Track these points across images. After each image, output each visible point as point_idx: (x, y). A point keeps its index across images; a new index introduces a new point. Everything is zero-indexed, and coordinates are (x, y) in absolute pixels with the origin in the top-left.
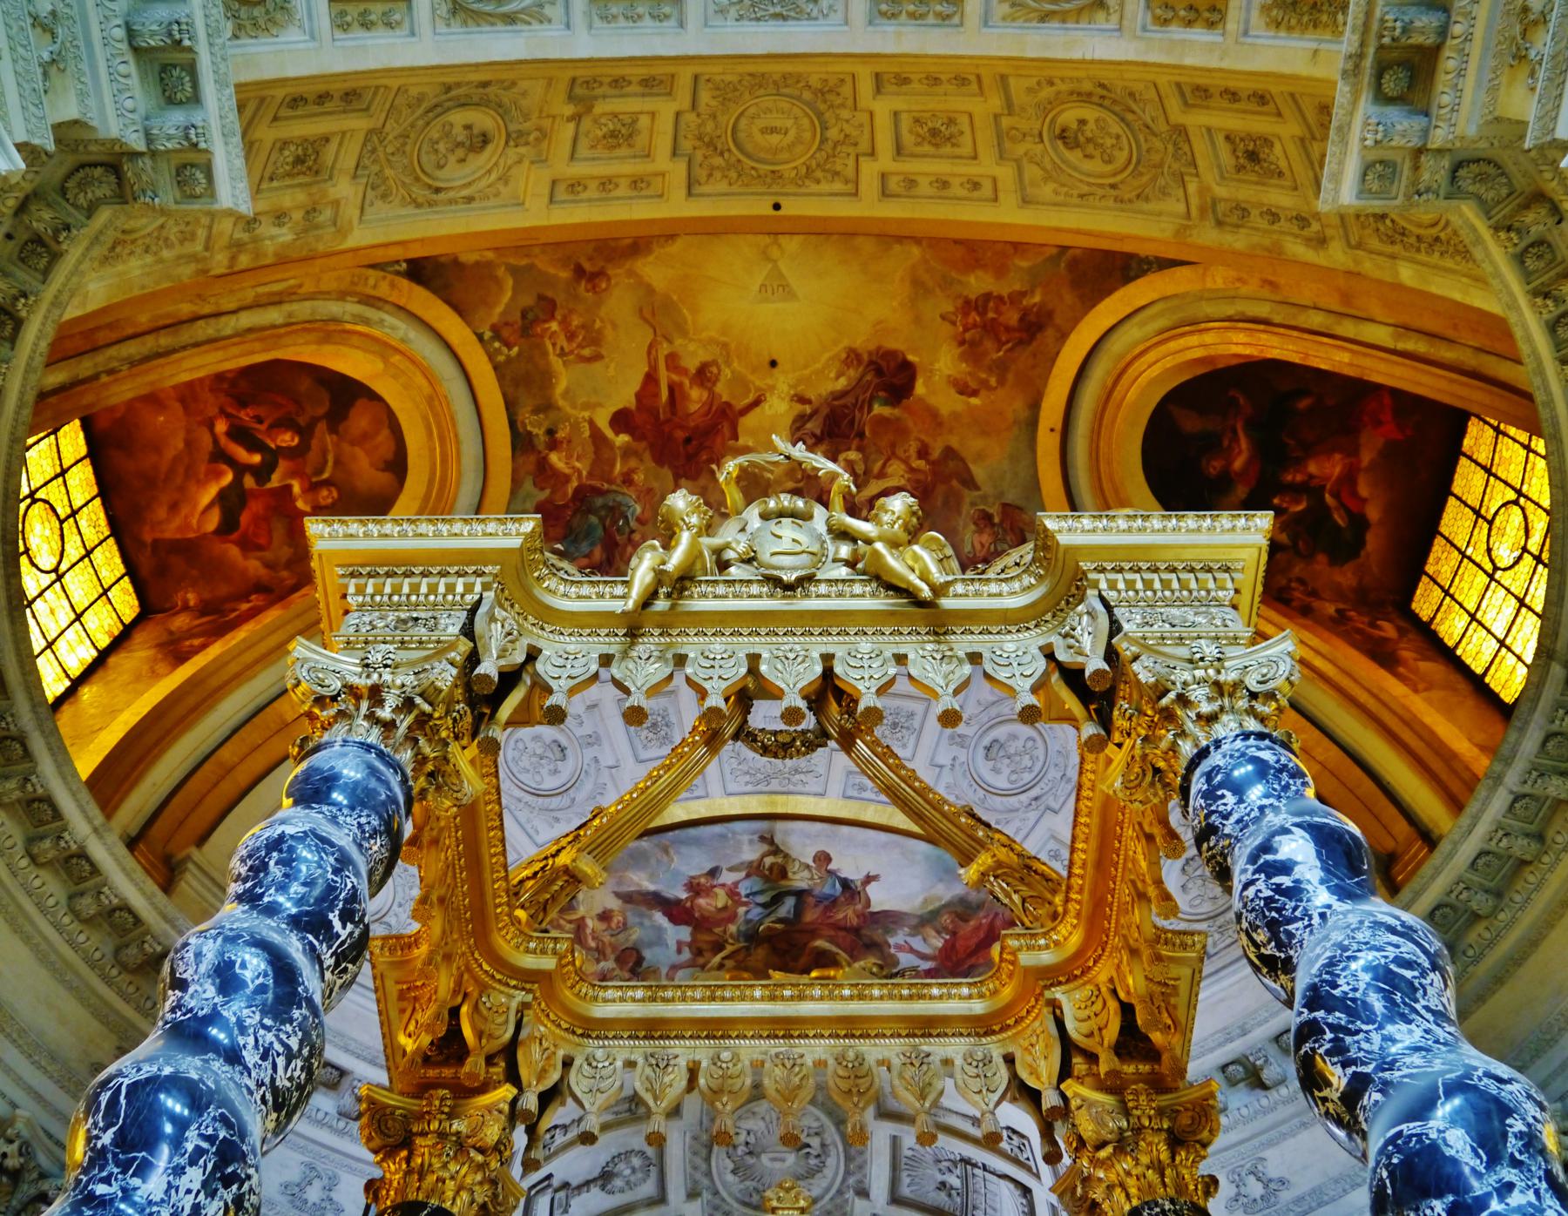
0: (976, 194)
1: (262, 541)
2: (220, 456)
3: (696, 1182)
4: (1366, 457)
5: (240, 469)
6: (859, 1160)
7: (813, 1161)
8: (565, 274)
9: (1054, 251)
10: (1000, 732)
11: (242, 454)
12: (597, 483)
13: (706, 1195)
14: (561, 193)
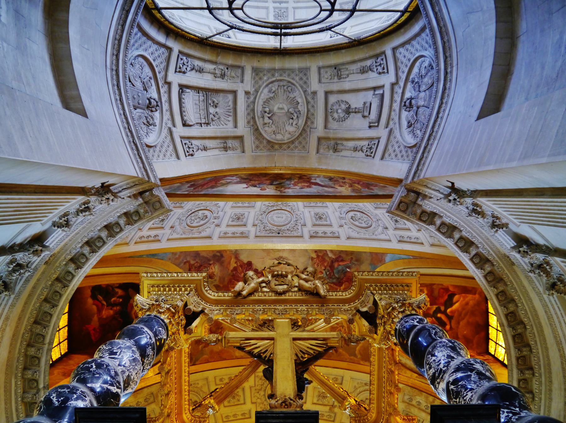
0: (221, 377)
1: (442, 290)
2: (450, 318)
3: (313, 99)
4: (96, 318)
5: (444, 312)
6: (249, 117)
7: (267, 110)
8: (340, 350)
9: (197, 363)
10: (202, 222)
11: (443, 317)
12: (334, 286)
13: (309, 91)
14: (340, 378)
